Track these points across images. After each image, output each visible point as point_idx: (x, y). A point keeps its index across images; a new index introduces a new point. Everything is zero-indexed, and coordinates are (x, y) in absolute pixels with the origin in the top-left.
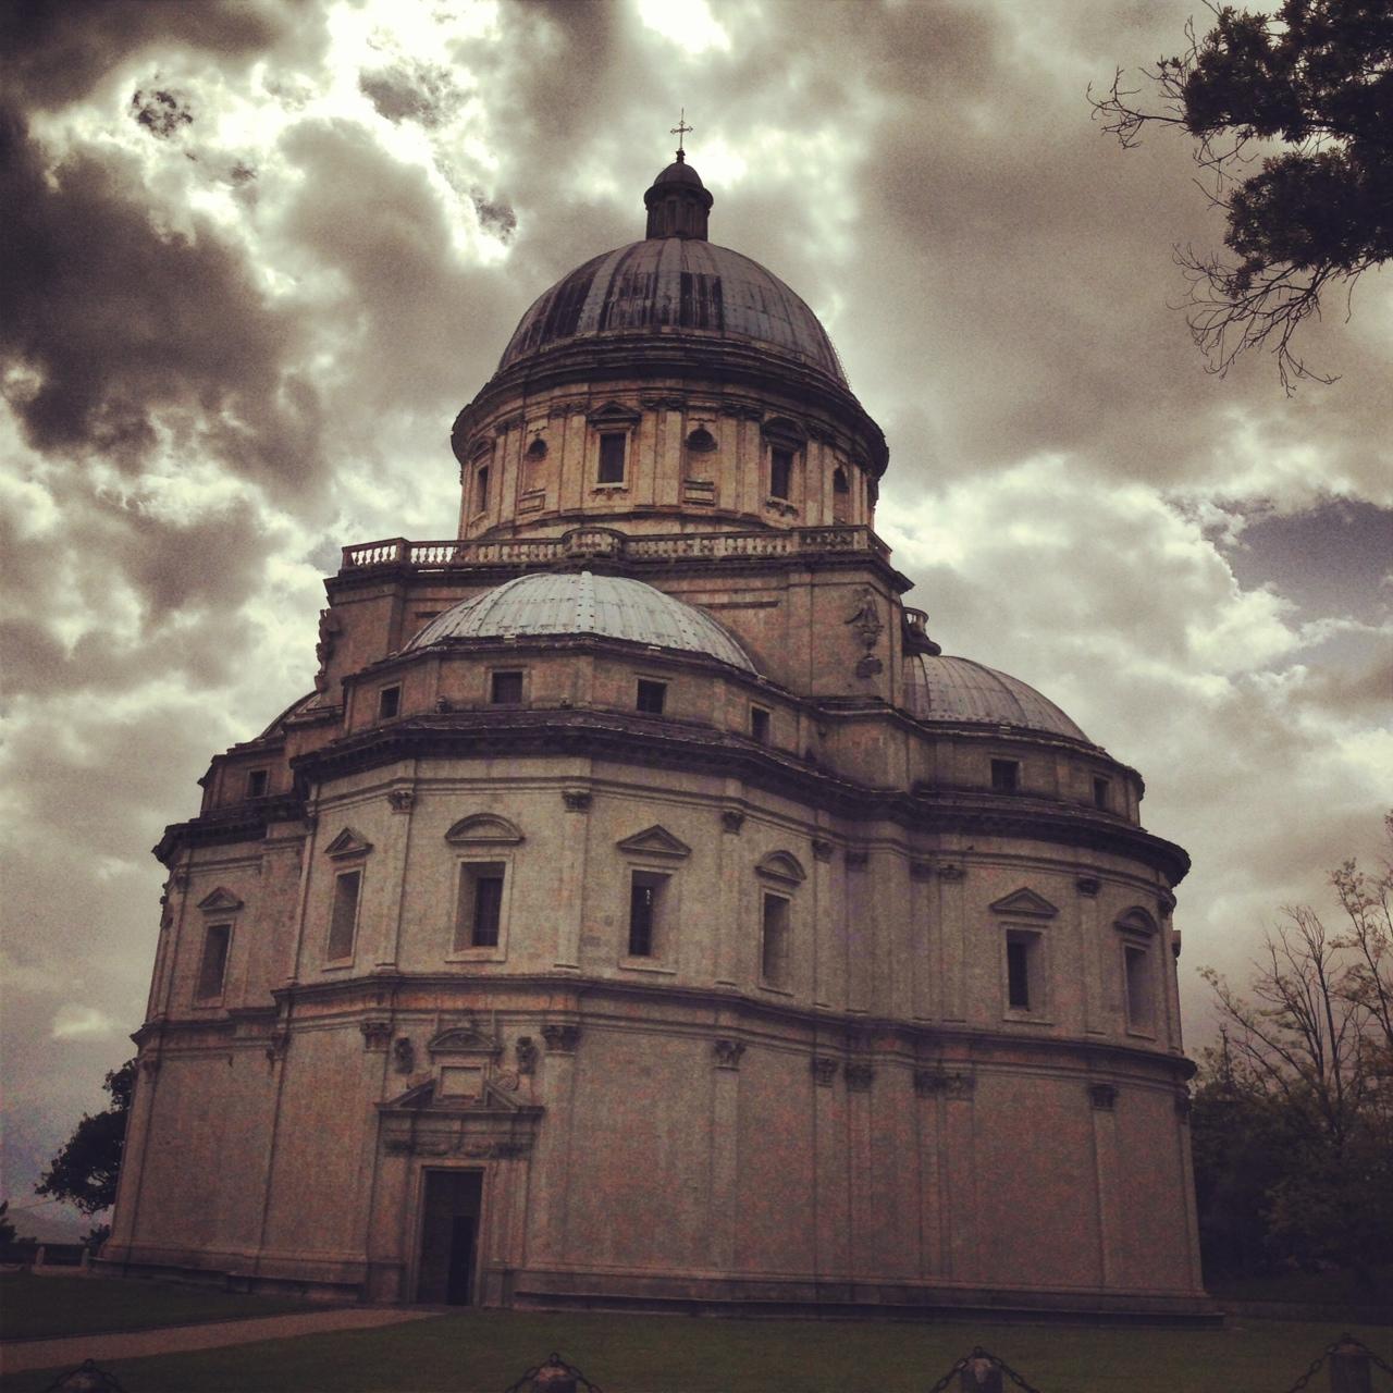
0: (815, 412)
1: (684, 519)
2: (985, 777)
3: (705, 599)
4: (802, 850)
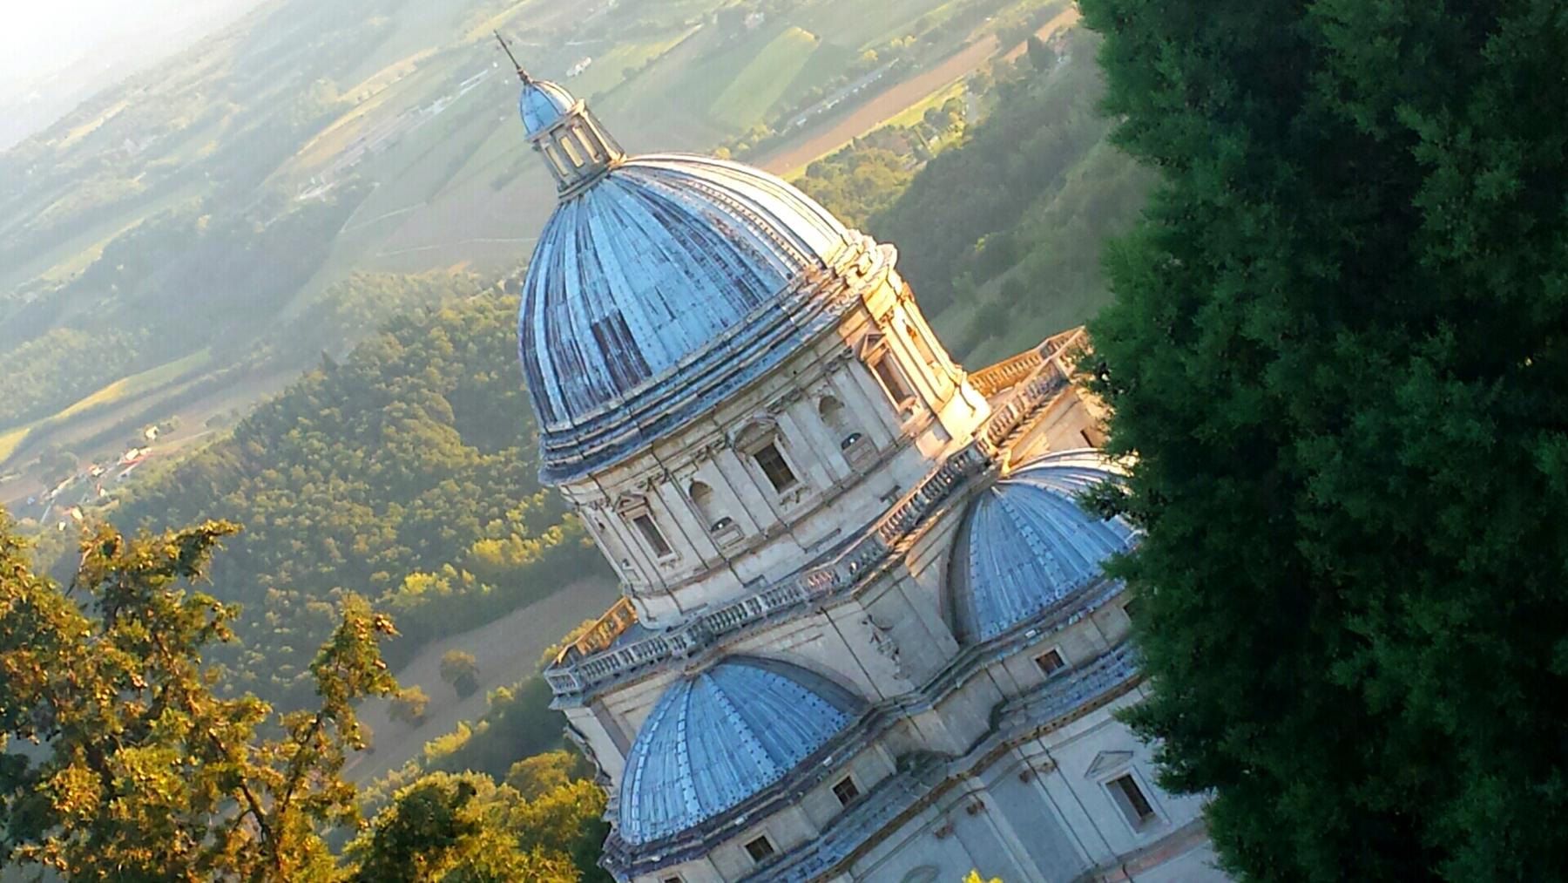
0: (767, 389)
1: (730, 564)
2: (1041, 674)
3: (777, 647)
4: (926, 850)
